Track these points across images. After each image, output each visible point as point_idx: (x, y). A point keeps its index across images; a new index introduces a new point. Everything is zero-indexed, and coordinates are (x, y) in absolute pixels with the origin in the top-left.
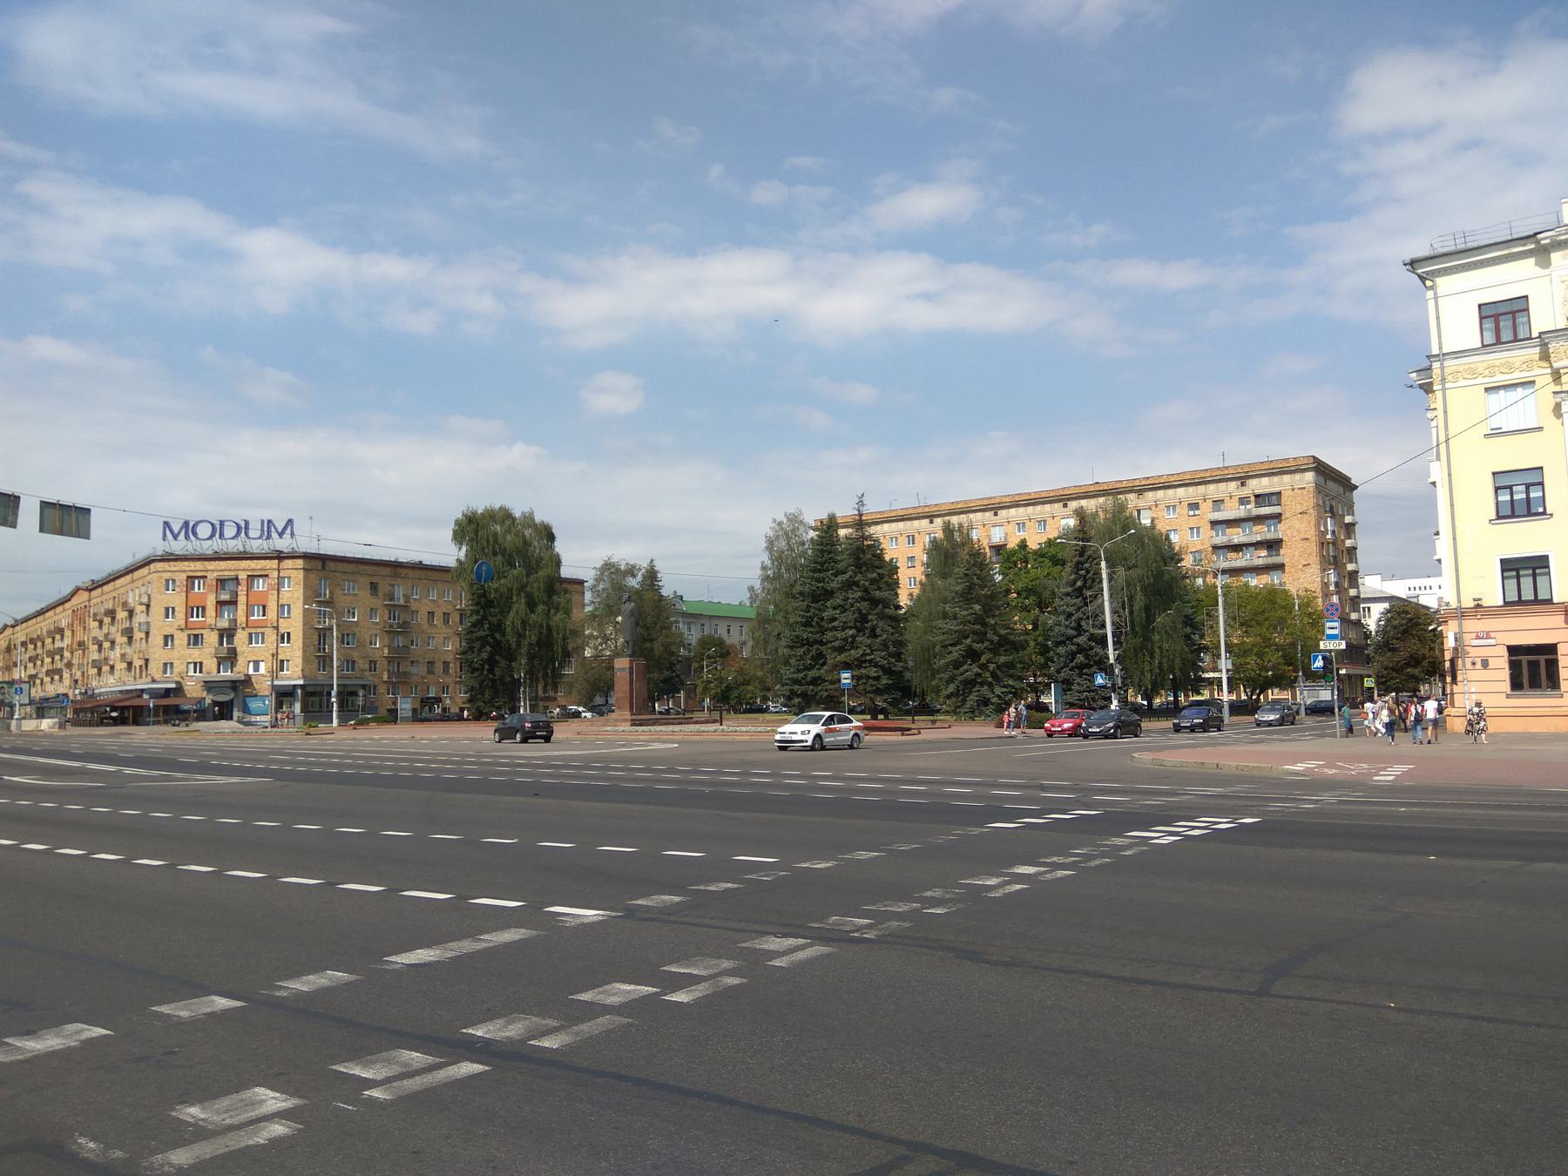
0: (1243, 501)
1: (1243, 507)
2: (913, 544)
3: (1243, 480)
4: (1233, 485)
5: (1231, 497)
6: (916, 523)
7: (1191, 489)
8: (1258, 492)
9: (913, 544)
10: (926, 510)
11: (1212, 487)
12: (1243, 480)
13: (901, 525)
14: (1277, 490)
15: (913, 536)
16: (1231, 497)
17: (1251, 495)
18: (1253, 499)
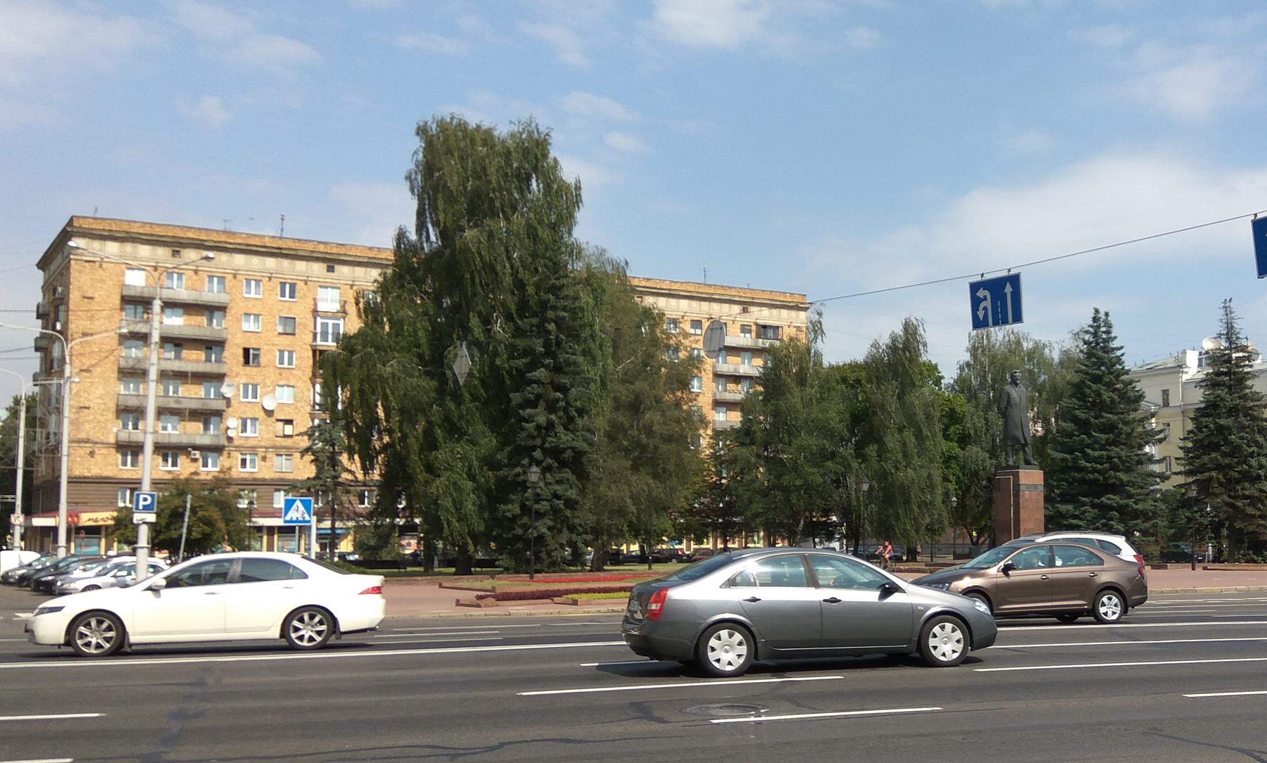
0: (745, 329)
1: (743, 335)
2: (292, 296)
3: (746, 306)
4: (736, 309)
5: (733, 321)
6: (301, 266)
7: (694, 304)
8: (761, 322)
9: (292, 296)
10: (321, 248)
11: (715, 306)
12: (746, 306)
13: (271, 263)
14: (776, 323)
15: (293, 286)
16: (733, 321)
17: (752, 324)
18: (754, 328)
